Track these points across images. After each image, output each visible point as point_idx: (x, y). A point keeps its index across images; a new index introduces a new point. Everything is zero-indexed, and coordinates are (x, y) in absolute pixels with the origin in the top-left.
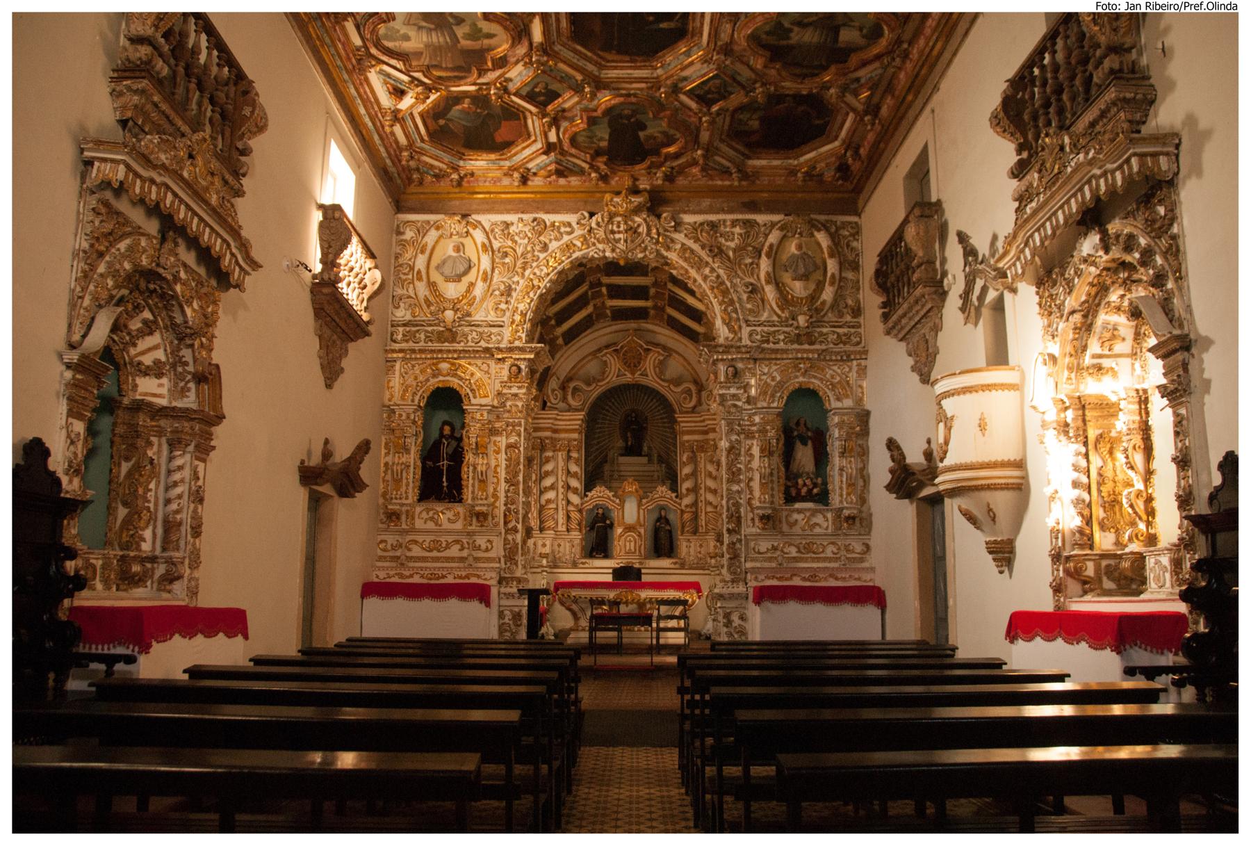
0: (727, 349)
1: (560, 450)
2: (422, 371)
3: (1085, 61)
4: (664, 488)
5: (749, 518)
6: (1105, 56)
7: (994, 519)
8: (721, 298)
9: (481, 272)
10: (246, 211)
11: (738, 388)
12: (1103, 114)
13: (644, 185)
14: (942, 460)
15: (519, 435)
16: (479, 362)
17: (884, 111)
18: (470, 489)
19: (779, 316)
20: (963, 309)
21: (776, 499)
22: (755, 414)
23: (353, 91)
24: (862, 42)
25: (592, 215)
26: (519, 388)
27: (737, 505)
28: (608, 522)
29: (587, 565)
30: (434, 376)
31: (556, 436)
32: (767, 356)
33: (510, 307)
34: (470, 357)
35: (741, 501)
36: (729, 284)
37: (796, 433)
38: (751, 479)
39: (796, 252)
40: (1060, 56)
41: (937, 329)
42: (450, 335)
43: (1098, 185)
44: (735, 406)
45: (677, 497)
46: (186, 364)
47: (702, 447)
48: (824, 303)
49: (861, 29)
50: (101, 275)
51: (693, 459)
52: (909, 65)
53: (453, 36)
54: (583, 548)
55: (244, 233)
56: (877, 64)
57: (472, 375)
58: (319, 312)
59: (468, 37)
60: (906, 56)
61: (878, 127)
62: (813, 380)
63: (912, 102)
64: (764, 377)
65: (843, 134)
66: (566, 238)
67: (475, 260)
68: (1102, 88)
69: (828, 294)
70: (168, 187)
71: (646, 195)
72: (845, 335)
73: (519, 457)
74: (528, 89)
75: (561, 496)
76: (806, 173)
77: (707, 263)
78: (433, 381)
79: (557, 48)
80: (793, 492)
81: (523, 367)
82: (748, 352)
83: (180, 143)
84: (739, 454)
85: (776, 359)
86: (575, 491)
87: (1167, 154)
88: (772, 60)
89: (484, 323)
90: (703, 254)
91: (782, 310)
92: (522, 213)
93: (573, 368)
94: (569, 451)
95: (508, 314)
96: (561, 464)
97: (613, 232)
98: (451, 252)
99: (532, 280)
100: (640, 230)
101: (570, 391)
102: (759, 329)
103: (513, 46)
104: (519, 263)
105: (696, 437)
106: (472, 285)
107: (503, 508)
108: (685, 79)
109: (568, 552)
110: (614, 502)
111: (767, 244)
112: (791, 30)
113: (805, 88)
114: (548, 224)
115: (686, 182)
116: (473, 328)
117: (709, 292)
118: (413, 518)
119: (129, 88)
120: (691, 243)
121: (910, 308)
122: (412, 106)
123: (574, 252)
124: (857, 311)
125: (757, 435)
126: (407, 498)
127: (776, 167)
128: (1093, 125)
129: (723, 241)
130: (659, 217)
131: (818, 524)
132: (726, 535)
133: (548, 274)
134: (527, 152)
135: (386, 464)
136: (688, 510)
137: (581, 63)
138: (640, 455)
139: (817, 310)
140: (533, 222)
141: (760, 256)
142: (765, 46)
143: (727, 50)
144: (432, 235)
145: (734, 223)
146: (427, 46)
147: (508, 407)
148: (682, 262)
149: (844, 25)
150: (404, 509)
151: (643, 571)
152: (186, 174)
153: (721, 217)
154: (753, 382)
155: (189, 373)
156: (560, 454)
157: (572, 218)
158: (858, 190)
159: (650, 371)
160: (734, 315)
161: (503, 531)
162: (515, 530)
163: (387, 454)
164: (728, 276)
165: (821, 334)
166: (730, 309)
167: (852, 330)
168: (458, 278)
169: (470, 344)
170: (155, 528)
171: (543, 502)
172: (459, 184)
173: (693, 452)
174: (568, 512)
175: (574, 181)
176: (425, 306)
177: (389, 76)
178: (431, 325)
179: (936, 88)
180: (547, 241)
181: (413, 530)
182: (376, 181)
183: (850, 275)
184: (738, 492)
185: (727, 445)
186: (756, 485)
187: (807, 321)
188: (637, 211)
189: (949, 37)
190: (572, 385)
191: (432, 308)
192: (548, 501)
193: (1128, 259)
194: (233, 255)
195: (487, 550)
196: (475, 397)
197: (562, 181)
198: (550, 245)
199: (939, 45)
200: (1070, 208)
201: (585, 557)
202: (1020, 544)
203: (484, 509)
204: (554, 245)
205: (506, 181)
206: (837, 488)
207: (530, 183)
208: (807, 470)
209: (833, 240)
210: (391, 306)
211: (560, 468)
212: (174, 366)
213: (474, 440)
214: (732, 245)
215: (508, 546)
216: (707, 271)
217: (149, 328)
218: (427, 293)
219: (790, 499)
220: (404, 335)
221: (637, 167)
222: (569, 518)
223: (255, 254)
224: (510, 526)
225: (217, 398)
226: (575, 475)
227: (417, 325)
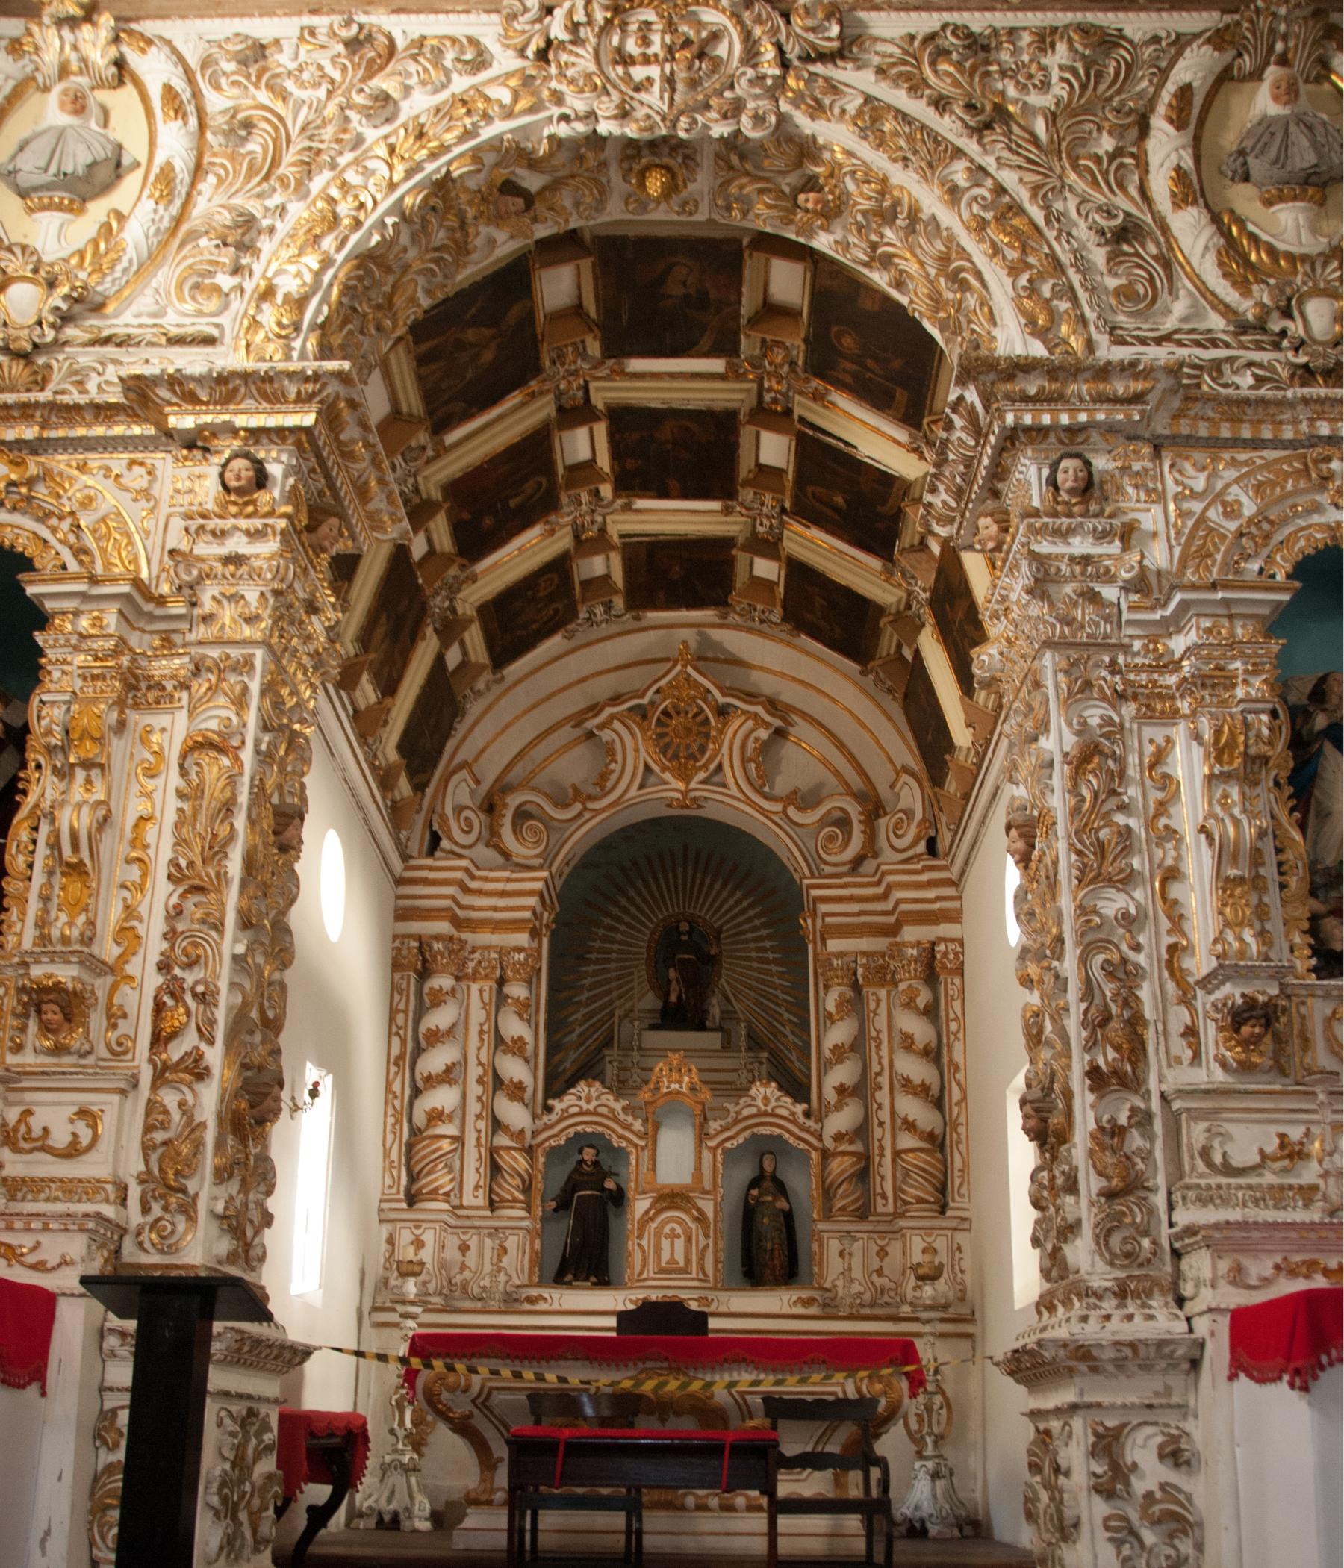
1: (474, 977)
5: (1176, 1027)
8: (1012, 255)
9: (155, 170)
11: (1102, 536)
15: (240, 702)
16: (118, 461)
18: (34, 906)
19: (1226, 310)
22: (1173, 625)
26: (255, 535)
27: (1124, 974)
28: (609, 1184)
31: (466, 936)
32: (1203, 431)
33: (249, 286)
35: (1141, 959)
36: (1037, 214)
38: (1172, 874)
45: (807, 1114)
47: (883, 968)
51: (855, 1004)
57: (87, 503)
64: (1197, 507)
66: (461, 83)
67: (135, 149)
73: (232, 781)
75: (474, 1108)
77: (958, 153)
84: (1122, 774)
85: (1236, 443)
86: (516, 1091)
89: (148, 334)
91: (1243, 286)
92: (314, 12)
93: (520, 755)
94: (501, 982)
95: (237, 305)
96: (477, 1015)
97: (625, 60)
99: (332, 201)
100: (721, 50)
101: (507, 821)
105: (864, 944)
107: (154, 981)
109: (488, 1268)
110: (627, 1127)
111: (1170, 88)
114: (401, 43)
116: (110, 350)
117: (968, 241)
120: (899, 97)
123: (486, 117)
125: (1184, 705)
129: (1012, 91)
132: (1083, 1100)
133: (392, 186)
136: (844, 1147)
138: (701, 1027)
141: (1144, 129)
145: (1045, 39)
148: (867, 152)
153: (1002, 19)
154: (1150, 519)
156: (475, 988)
159: (734, 774)
160: (1063, 305)
164: (1035, 190)
166: (1046, 290)
171: (419, 1119)
173: (856, 987)
174: (493, 1151)
184: (1127, 920)
185: (1070, 741)
190: (514, 801)
192: (436, 1116)
201: (540, 1284)
203: (66, 974)
204: (418, 104)
211: (474, 1030)
213: (58, 713)
215: (159, 1136)
224: (176, 1051)
226: (517, 1047)
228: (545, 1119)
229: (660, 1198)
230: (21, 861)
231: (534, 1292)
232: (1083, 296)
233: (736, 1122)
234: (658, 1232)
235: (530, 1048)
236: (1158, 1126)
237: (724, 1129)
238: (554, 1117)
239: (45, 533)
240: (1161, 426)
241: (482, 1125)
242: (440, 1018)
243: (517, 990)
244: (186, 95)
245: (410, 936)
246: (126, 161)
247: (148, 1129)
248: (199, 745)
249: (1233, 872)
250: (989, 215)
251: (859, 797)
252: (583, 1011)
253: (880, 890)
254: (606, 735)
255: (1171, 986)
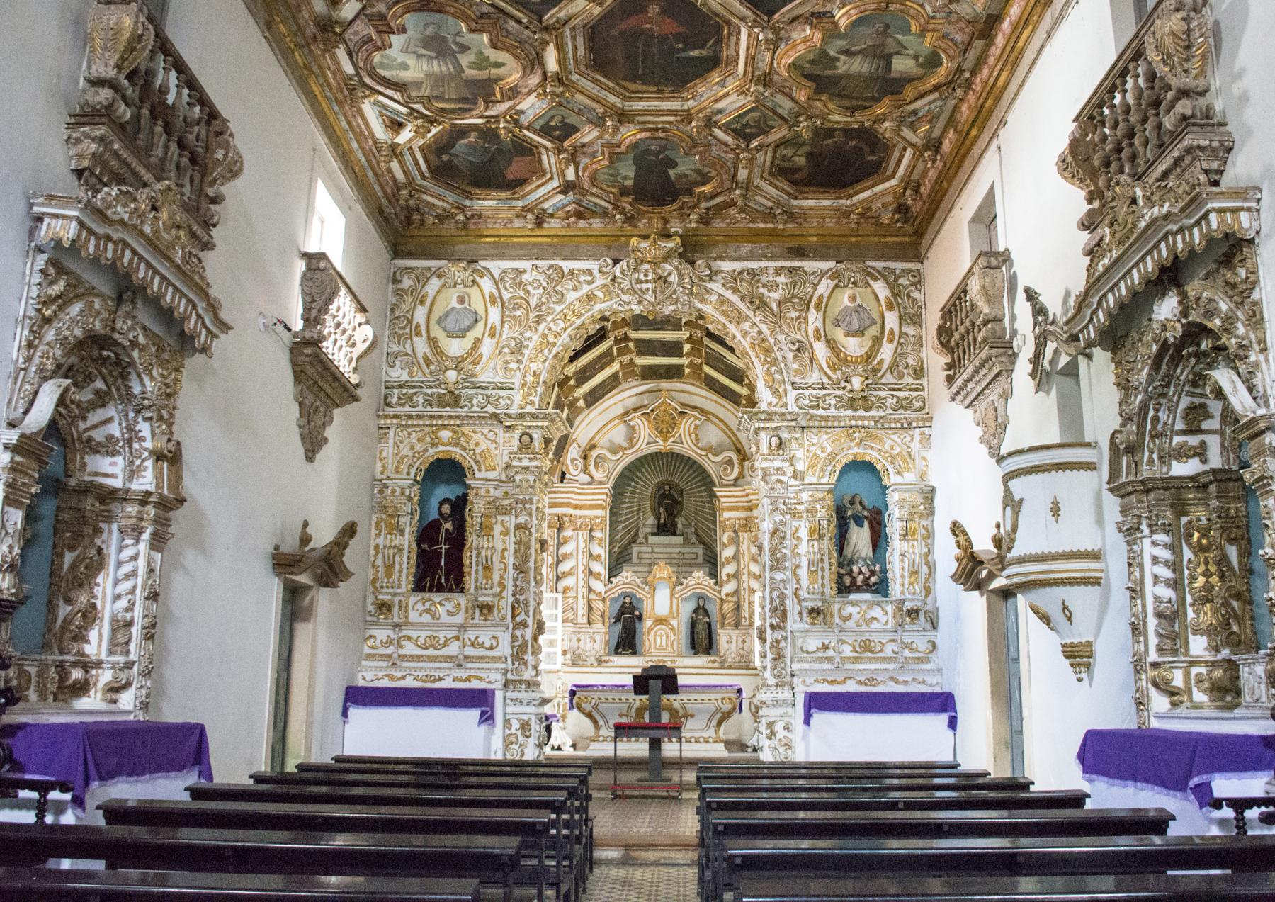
0: (770, 416)
1: (580, 529)
2: (419, 440)
3: (1156, 104)
4: (701, 574)
5: (796, 612)
6: (1177, 99)
7: (1069, 619)
8: (763, 357)
10: (215, 266)
12: (1177, 162)
13: (675, 227)
14: (1010, 549)
15: (530, 514)
16: (485, 431)
17: (946, 146)
18: (473, 576)
19: (829, 377)
20: (1033, 375)
21: (827, 589)
22: (802, 491)
23: (344, 124)
24: (920, 71)
25: (616, 261)
27: (782, 597)
28: (637, 613)
29: (609, 664)
30: (433, 445)
32: (817, 424)
33: (522, 367)
34: (474, 424)
35: (786, 592)
36: (772, 341)
37: (849, 513)
38: (798, 567)
39: (849, 304)
40: (1130, 98)
41: (1006, 396)
42: (453, 399)
43: (1175, 242)
44: (780, 481)
45: (716, 584)
46: (143, 439)
48: (882, 361)
49: (916, 58)
50: (48, 344)
51: (735, 541)
52: (972, 97)
53: (458, 64)
54: (607, 643)
55: (213, 292)
56: (935, 95)
57: (477, 444)
58: (299, 374)
59: (474, 66)
60: (968, 85)
61: (939, 164)
62: (870, 451)
63: (977, 137)
65: (901, 171)
66: (586, 288)
67: (481, 312)
68: (1176, 136)
69: (887, 352)
70: (126, 244)
71: (678, 239)
72: (906, 399)
74: (541, 122)
75: (581, 583)
76: (861, 215)
77: (748, 316)
78: (431, 451)
79: (574, 77)
80: (847, 581)
81: (535, 436)
82: (795, 420)
83: (143, 194)
84: (784, 537)
87: (1249, 210)
88: (818, 91)
90: (742, 306)
91: (834, 370)
94: (591, 530)
96: (582, 545)
97: (640, 282)
98: (454, 304)
99: (546, 335)
100: (671, 279)
102: (806, 392)
103: (524, 75)
104: (532, 317)
106: (478, 341)
107: (511, 599)
108: (720, 111)
110: (643, 589)
111: (816, 295)
112: (837, 59)
113: (855, 121)
114: (566, 272)
115: (723, 225)
117: (749, 350)
118: (406, 611)
119: (86, 135)
120: (728, 294)
121: (976, 372)
122: (411, 140)
124: (919, 372)
125: (804, 515)
126: (400, 587)
127: (826, 208)
128: (1166, 174)
130: (692, 263)
131: (876, 619)
132: (769, 632)
134: (542, 191)
135: (377, 547)
136: (730, 598)
137: (603, 94)
138: (674, 534)
139: (874, 371)
140: (548, 269)
142: (808, 77)
143: (766, 80)
144: (434, 285)
145: (778, 272)
146: (428, 75)
147: (518, 482)
149: (897, 53)
150: (397, 599)
151: (677, 671)
152: (148, 230)
153: (763, 264)
154: (800, 453)
155: (146, 450)
156: (580, 533)
157: (593, 265)
158: (919, 234)
160: (778, 377)
161: (511, 626)
162: (524, 625)
163: (378, 535)
165: (880, 398)
167: (914, 394)
168: (462, 334)
169: (475, 409)
170: (101, 627)
172: (465, 224)
173: (735, 532)
174: (589, 602)
175: (596, 223)
176: (424, 366)
177: (385, 107)
178: (430, 387)
179: (1002, 122)
180: (564, 292)
181: (407, 624)
182: (369, 224)
183: (910, 330)
184: (783, 581)
185: (771, 527)
186: (803, 573)
187: (862, 383)
188: (666, 258)
189: (1015, 65)
190: (595, 453)
191: (433, 367)
193: (1210, 325)
194: (199, 316)
195: (491, 648)
196: (480, 470)
197: (582, 224)
198: (568, 296)
199: (1004, 74)
200: (1146, 266)
201: (609, 654)
202: (1099, 649)
203: (488, 599)
204: (572, 296)
205: (518, 223)
206: (898, 576)
207: (545, 225)
208: (863, 555)
209: (892, 289)
210: (384, 365)
212: (129, 442)
213: (478, 520)
214: (775, 296)
216: (746, 326)
217: (101, 400)
218: (427, 350)
219: (845, 587)
220: (400, 398)
221: (668, 208)
222: (590, 608)
223: (223, 315)
224: (519, 619)
225: (176, 480)
226: (597, 558)
227: (414, 387)
228: (610, 586)
229: (657, 621)
230: (468, 561)
231: (607, 658)
232: (784, 372)
233: (687, 587)
234: (655, 635)
235: (603, 558)
236: (789, 640)
237: (682, 590)
238: (613, 585)
239: (464, 454)
240: (803, 423)
241: (585, 590)
242: (566, 549)
243: (598, 534)
244: (497, 295)
245: (555, 515)
246: (479, 318)
247: (512, 642)
248: (518, 527)
249: (813, 569)
250: (756, 342)
251: (739, 451)
252: (623, 525)
253: (743, 493)
254: (632, 423)
255: (795, 600)
